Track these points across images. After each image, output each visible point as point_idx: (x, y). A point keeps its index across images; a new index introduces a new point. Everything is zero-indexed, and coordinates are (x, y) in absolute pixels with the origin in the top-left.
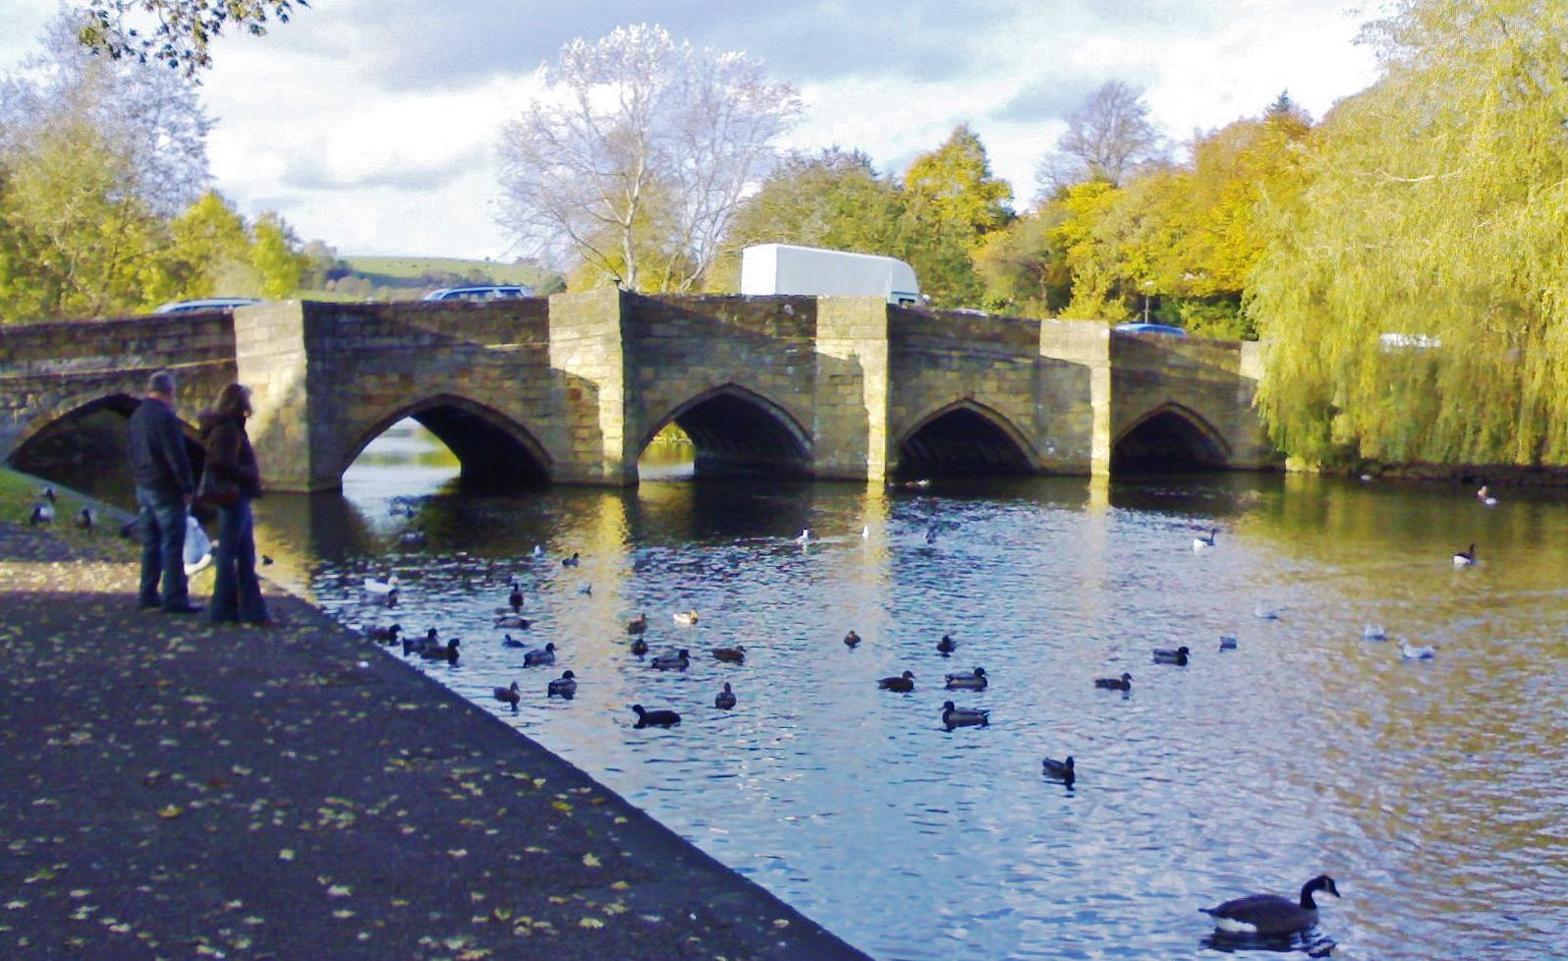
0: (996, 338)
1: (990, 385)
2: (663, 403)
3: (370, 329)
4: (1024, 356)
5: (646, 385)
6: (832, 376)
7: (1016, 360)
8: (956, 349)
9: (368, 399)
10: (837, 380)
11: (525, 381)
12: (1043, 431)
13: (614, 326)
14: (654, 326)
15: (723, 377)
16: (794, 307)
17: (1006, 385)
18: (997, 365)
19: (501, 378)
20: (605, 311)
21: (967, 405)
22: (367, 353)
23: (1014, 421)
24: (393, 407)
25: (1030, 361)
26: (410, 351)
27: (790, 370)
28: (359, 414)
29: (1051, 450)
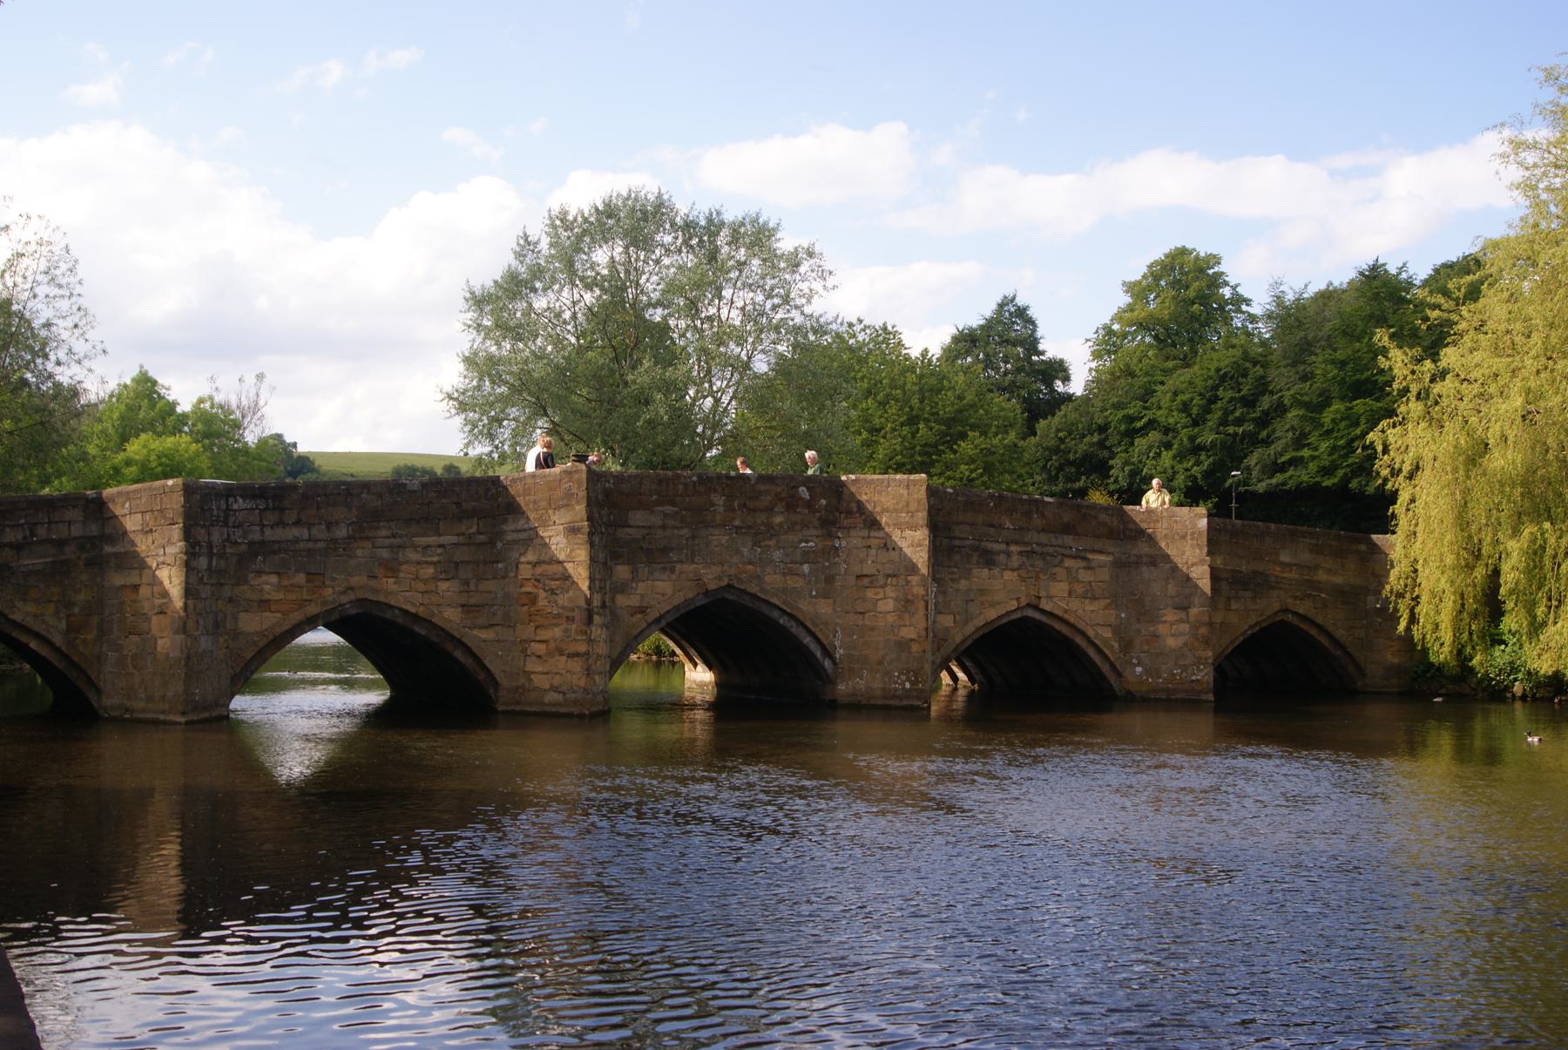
0: (1067, 529)
1: (1060, 588)
2: (642, 610)
3: (271, 518)
4: (1101, 552)
5: (623, 588)
6: (859, 577)
7: (1090, 556)
9: (264, 604)
10: (866, 581)
11: (467, 583)
12: (1127, 646)
13: (580, 509)
14: (631, 514)
15: (720, 578)
16: (809, 489)
17: (1079, 589)
18: (1068, 563)
19: (436, 579)
20: (569, 495)
21: (1030, 613)
22: (261, 549)
23: (1091, 633)
24: (297, 616)
25: (1110, 558)
26: (321, 545)
27: (806, 568)
28: (254, 623)
29: (1139, 669)
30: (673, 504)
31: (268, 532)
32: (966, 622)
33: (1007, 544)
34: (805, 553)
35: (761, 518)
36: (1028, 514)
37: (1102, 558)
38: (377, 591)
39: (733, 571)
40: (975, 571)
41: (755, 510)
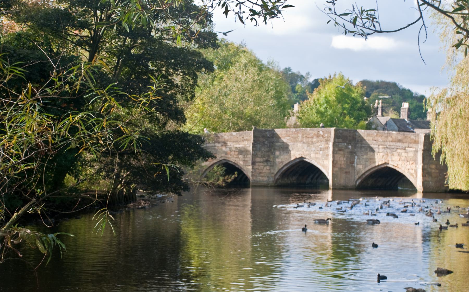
1: (396, 158)
2: (282, 162)
8: (382, 145)
11: (244, 156)
15: (299, 155)
18: (399, 151)
25: (414, 149)
27: (321, 152)
30: (289, 136)
31: (207, 144)
32: (366, 167)
33: (379, 145)
34: (321, 148)
35: (310, 140)
36: (387, 137)
37: (411, 149)
38: (227, 157)
39: (302, 153)
40: (369, 153)
41: (309, 138)
